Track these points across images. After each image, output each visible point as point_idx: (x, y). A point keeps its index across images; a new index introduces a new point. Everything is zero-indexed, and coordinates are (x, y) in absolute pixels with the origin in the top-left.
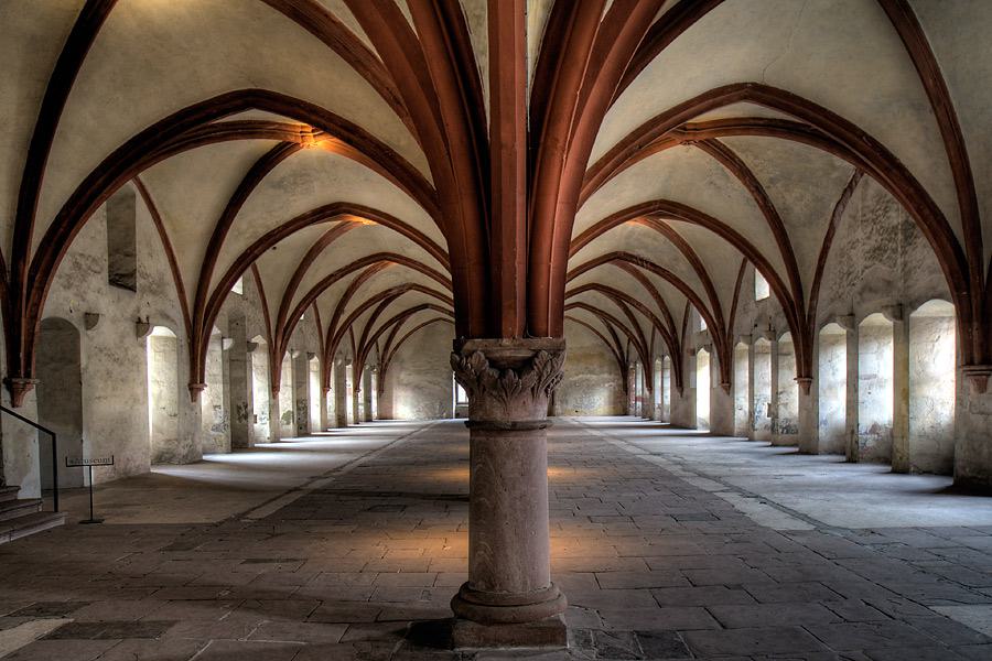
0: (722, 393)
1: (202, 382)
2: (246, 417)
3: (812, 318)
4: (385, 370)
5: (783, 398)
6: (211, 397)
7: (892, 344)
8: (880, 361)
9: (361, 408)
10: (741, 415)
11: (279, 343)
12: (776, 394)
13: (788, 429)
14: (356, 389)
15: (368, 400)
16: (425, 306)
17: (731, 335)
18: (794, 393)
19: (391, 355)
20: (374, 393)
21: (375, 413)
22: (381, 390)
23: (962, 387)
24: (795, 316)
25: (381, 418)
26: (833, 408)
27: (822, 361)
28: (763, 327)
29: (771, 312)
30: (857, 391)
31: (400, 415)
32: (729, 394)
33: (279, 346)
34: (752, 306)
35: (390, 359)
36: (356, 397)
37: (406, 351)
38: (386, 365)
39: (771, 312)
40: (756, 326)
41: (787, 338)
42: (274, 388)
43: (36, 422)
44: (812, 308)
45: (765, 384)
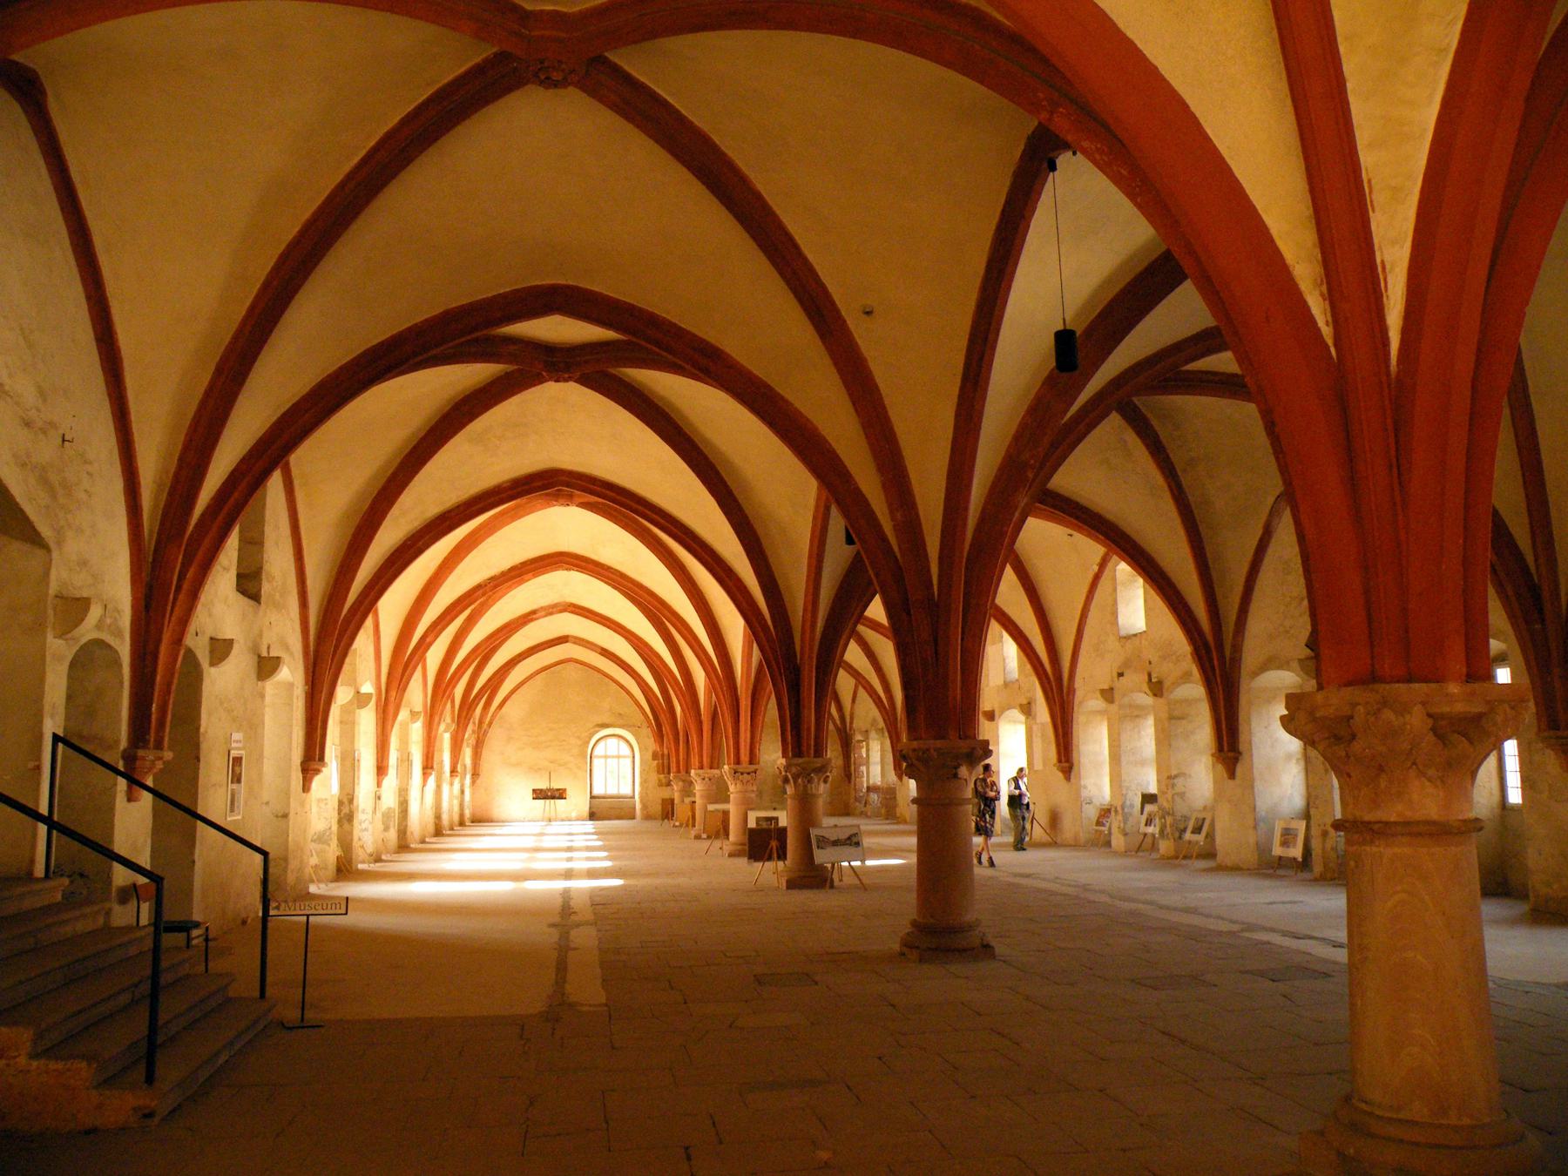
1: (322, 758)
3: (1236, 661)
6: (391, 781)
11: (393, 694)
16: (562, 640)
19: (494, 716)
20: (468, 777)
21: (467, 813)
22: (475, 774)
24: (1211, 660)
27: (1254, 724)
28: (1136, 679)
31: (504, 816)
32: (1068, 778)
37: (514, 711)
38: (486, 733)
40: (1121, 675)
41: (1195, 690)
42: (381, 770)
43: (199, 823)
44: (1237, 648)
45: (1143, 763)
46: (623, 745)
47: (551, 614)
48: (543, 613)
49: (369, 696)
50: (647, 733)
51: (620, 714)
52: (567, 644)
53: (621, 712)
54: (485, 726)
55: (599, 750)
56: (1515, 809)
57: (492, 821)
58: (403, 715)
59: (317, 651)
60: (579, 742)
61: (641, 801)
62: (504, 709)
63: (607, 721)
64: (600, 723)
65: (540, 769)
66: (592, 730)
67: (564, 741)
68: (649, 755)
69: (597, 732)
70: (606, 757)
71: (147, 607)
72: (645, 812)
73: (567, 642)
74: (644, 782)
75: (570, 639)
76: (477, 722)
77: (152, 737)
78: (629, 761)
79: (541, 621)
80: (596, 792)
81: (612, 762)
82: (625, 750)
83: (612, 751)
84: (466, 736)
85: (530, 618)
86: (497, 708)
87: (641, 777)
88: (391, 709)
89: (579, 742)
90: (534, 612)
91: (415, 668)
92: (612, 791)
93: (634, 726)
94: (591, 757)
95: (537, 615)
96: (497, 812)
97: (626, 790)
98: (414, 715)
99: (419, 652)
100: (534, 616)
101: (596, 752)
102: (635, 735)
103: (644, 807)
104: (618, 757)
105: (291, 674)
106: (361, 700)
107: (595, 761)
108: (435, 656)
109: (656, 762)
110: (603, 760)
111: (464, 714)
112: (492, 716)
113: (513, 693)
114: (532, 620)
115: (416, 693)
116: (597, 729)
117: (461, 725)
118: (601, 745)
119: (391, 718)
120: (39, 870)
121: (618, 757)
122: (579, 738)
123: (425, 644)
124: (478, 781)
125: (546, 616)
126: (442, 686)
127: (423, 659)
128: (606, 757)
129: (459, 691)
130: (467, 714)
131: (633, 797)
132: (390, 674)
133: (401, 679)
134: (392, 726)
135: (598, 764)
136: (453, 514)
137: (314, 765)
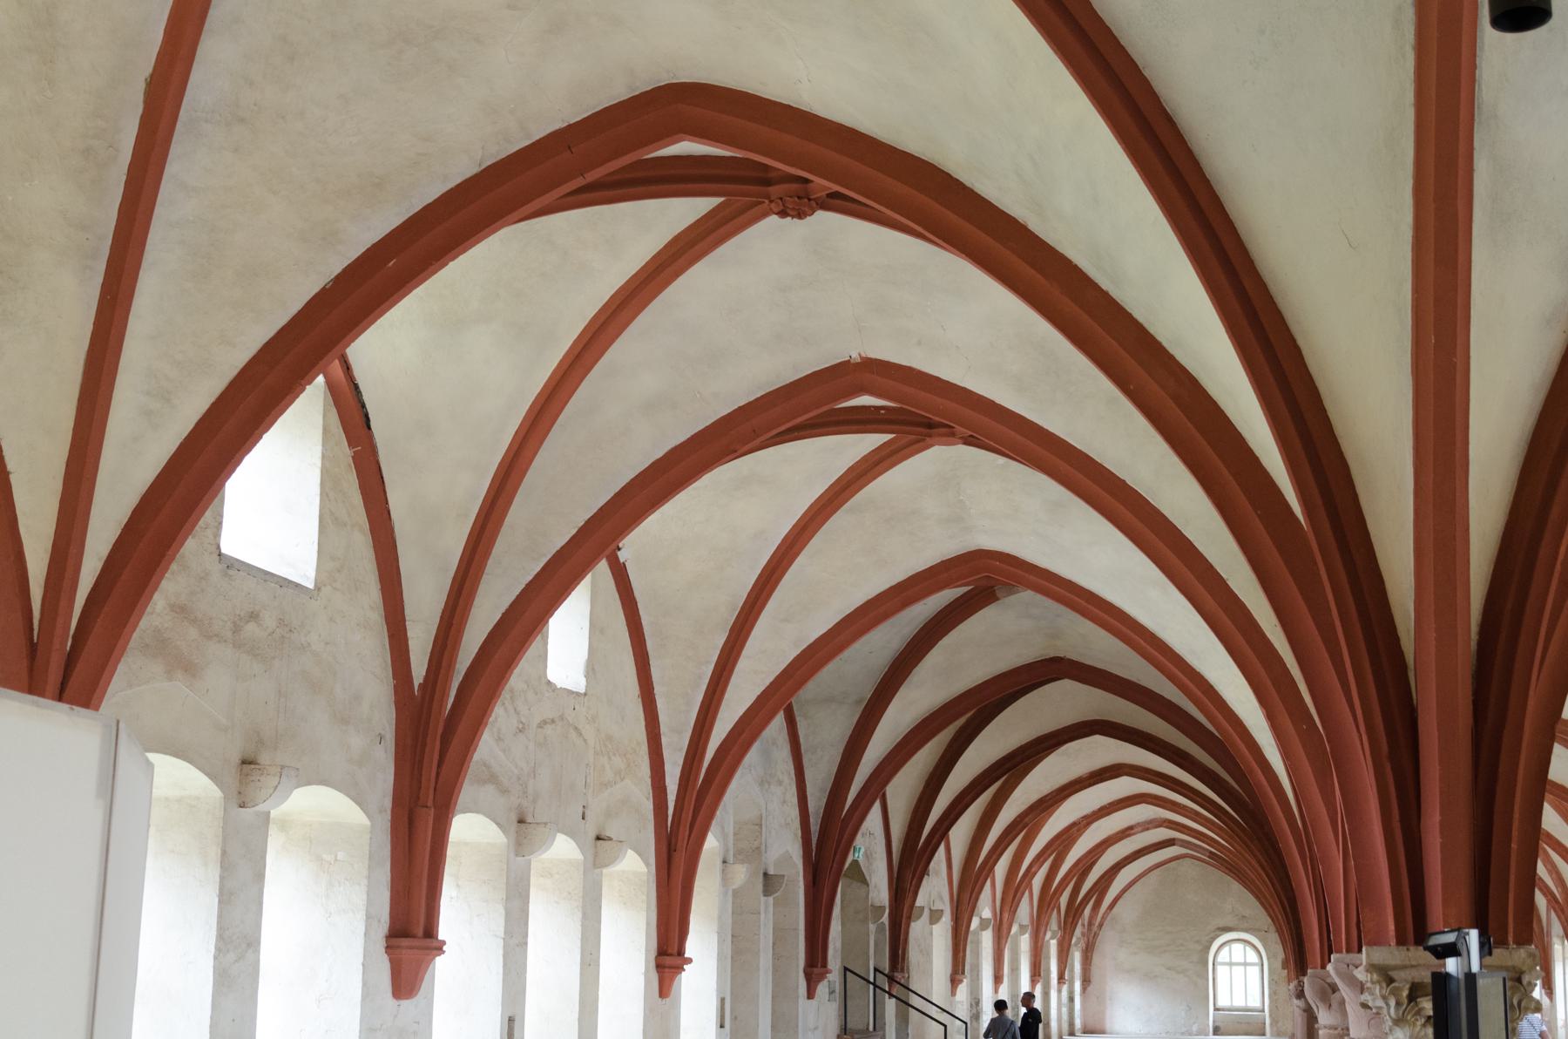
4: (1094, 944)
9: (1065, 1010)
11: (1006, 916)
14: (1061, 978)
15: (1071, 999)
16: (1170, 843)
19: (1103, 918)
20: (1078, 986)
21: (1078, 1023)
22: (1086, 981)
25: (1087, 1031)
33: (1005, 920)
35: (1101, 925)
36: (1059, 991)
37: (1127, 911)
46: (1249, 950)
47: (1148, 829)
48: (1140, 829)
49: (988, 920)
50: (1274, 937)
51: (1244, 917)
52: (1175, 847)
53: (1244, 914)
54: (1095, 928)
55: (1224, 956)
57: (1103, 1032)
58: (1015, 929)
59: (958, 901)
60: (1199, 947)
61: (1270, 1016)
62: (1115, 910)
63: (1230, 924)
64: (1221, 926)
65: (1156, 976)
66: (1212, 935)
67: (1182, 945)
68: (1278, 964)
69: (1218, 936)
70: (1231, 964)
71: (896, 901)
72: (1275, 1029)
73: (1174, 845)
74: (1273, 994)
75: (1176, 842)
76: (1086, 924)
77: (899, 966)
78: (1257, 969)
79: (1138, 835)
80: (1220, 1003)
81: (1238, 970)
82: (1252, 956)
83: (1238, 957)
84: (1073, 942)
85: (1128, 833)
86: (1108, 909)
87: (1270, 988)
88: (1005, 926)
89: (1199, 947)
90: (1131, 828)
91: (1023, 894)
92: (1239, 1002)
93: (1259, 930)
94: (1214, 964)
95: (1136, 830)
96: (1108, 1026)
97: (1255, 1002)
98: (1022, 928)
99: (1027, 880)
100: (1133, 831)
101: (1220, 959)
102: (1261, 940)
103: (1274, 1022)
104: (1245, 964)
105: (946, 920)
106: (984, 925)
107: (1220, 969)
108: (1037, 882)
109: (1286, 971)
110: (1227, 968)
111: (1071, 920)
112: (1103, 917)
113: (1124, 893)
114: (1129, 835)
115: (1025, 911)
116: (1218, 933)
117: (1068, 931)
118: (1225, 951)
119: (1005, 931)
120: (871, 1028)
121: (1245, 964)
122: (1198, 942)
123: (1030, 873)
124: (1089, 989)
125: (1142, 831)
126: (1047, 900)
127: (1030, 885)
128: (1231, 964)
129: (1064, 900)
130: (1073, 920)
131: (1263, 1011)
132: (1003, 900)
133: (1012, 903)
134: (1006, 942)
135: (1222, 972)
136: (1048, 798)
137: (958, 977)
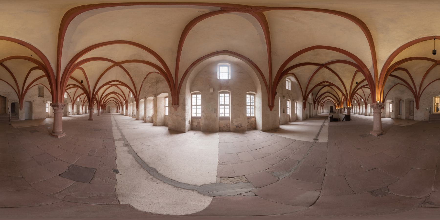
0: (127, 110)
2: (67, 112)
5: (134, 111)
7: (144, 104)
8: (150, 106)
10: (129, 113)
12: (133, 111)
13: (135, 116)
17: (128, 103)
18: (135, 110)
23: (170, 110)
26: (142, 113)
29: (132, 99)
30: (146, 110)
34: (130, 98)
39: (132, 99)
56: (166, 115)
